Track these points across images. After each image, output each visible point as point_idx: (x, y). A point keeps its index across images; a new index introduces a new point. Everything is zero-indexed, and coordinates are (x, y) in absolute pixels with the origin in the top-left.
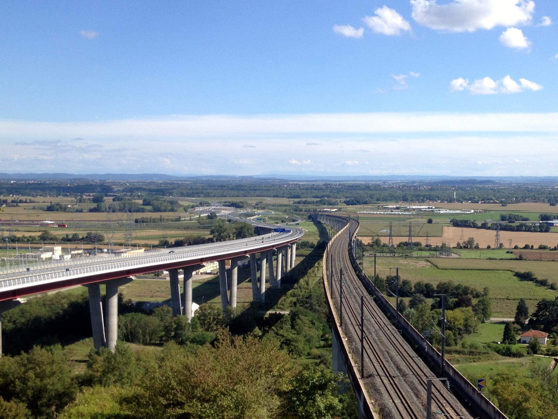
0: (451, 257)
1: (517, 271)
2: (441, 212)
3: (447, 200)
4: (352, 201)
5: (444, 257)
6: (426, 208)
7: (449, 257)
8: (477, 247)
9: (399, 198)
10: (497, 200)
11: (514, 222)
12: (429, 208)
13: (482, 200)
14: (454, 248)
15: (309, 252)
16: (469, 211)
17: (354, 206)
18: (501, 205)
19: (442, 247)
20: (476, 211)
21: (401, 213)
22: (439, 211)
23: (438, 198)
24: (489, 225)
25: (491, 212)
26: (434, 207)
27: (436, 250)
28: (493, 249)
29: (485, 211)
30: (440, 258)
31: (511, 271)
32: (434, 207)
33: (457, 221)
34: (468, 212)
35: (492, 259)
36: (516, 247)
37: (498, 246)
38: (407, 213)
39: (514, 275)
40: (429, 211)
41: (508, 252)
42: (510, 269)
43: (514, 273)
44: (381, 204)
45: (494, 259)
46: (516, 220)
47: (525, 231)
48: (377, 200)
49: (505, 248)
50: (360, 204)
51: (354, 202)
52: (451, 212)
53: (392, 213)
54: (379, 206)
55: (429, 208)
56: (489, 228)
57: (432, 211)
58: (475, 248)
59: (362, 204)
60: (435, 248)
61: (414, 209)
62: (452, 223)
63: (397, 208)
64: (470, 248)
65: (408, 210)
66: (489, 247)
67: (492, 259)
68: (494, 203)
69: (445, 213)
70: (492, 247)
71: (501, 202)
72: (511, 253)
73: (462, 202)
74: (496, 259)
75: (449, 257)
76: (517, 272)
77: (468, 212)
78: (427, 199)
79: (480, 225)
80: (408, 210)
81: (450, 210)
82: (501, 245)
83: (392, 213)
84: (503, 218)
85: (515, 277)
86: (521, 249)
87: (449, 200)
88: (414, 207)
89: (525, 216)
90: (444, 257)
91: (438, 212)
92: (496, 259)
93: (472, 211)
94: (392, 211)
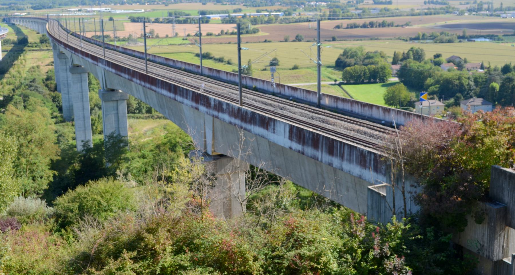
0: (138, 45)
3: (119, 3)
4: (38, 6)
5: (132, 45)
8: (157, 37)
9: (78, 3)
10: (160, 2)
11: (179, 17)
12: (106, 9)
13: (148, 2)
14: (138, 38)
15: (11, 48)
17: (41, 10)
18: (164, 5)
19: (128, 38)
21: (83, 14)
23: (111, 2)
24: (161, 20)
27: (124, 41)
29: (154, 10)
31: (191, 53)
32: (110, 9)
36: (188, 35)
37: (175, 34)
41: (183, 39)
43: (194, 55)
44: (64, 8)
46: (181, 16)
48: (60, 5)
49: (180, 37)
50: (45, 9)
51: (40, 7)
52: (126, 12)
53: (76, 14)
54: (62, 10)
55: (106, 9)
56: (161, 22)
57: (110, 12)
59: (48, 8)
60: (123, 39)
61: (94, 11)
62: (130, 20)
63: (80, 11)
64: (152, 38)
66: (167, 36)
68: (158, 4)
70: (170, 36)
71: (163, 3)
72: (186, 39)
73: (132, 4)
74: (176, 45)
75: (137, 45)
78: (102, 3)
79: (153, 20)
80: (89, 12)
81: (124, 10)
82: (177, 34)
84: (170, 14)
86: (192, 36)
87: (121, 3)
88: (94, 9)
89: (187, 12)
92: (176, 45)
93: (143, 11)
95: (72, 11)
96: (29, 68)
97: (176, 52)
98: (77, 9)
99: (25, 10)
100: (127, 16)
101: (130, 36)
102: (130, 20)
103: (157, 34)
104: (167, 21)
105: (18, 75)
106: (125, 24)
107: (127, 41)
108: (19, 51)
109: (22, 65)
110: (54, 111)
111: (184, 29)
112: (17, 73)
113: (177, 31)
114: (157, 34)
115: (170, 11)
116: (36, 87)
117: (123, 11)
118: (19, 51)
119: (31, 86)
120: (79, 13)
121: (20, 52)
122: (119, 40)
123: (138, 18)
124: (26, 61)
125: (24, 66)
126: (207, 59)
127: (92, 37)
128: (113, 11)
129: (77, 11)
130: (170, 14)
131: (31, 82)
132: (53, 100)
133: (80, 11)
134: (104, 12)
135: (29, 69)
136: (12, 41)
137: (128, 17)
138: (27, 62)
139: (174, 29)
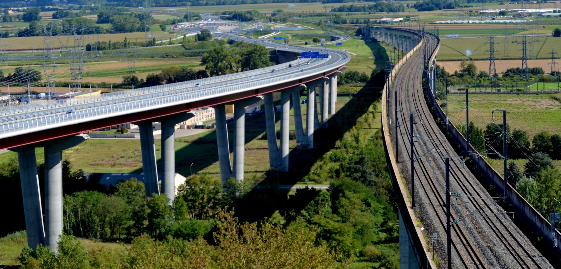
4: (427, 4)
6: (550, 12)
12: (555, 12)
15: (358, 89)
17: (431, 12)
21: (508, 21)
38: (518, 21)
50: (440, 9)
51: (431, 5)
53: (494, 21)
54: (471, 11)
55: (555, 12)
59: (444, 8)
61: (530, 15)
63: (502, 13)
65: (520, 16)
80: (520, 16)
83: (494, 21)
88: (530, 11)
94: (493, 19)
96: (376, 130)
98: (498, 12)
99: (403, 11)
105: (354, 144)
109: (366, 124)
112: (353, 139)
116: (364, 172)
119: (356, 171)
127: (508, 71)
129: (496, 14)
132: (390, 197)
133: (502, 13)
134: (549, 16)
136: (360, 75)
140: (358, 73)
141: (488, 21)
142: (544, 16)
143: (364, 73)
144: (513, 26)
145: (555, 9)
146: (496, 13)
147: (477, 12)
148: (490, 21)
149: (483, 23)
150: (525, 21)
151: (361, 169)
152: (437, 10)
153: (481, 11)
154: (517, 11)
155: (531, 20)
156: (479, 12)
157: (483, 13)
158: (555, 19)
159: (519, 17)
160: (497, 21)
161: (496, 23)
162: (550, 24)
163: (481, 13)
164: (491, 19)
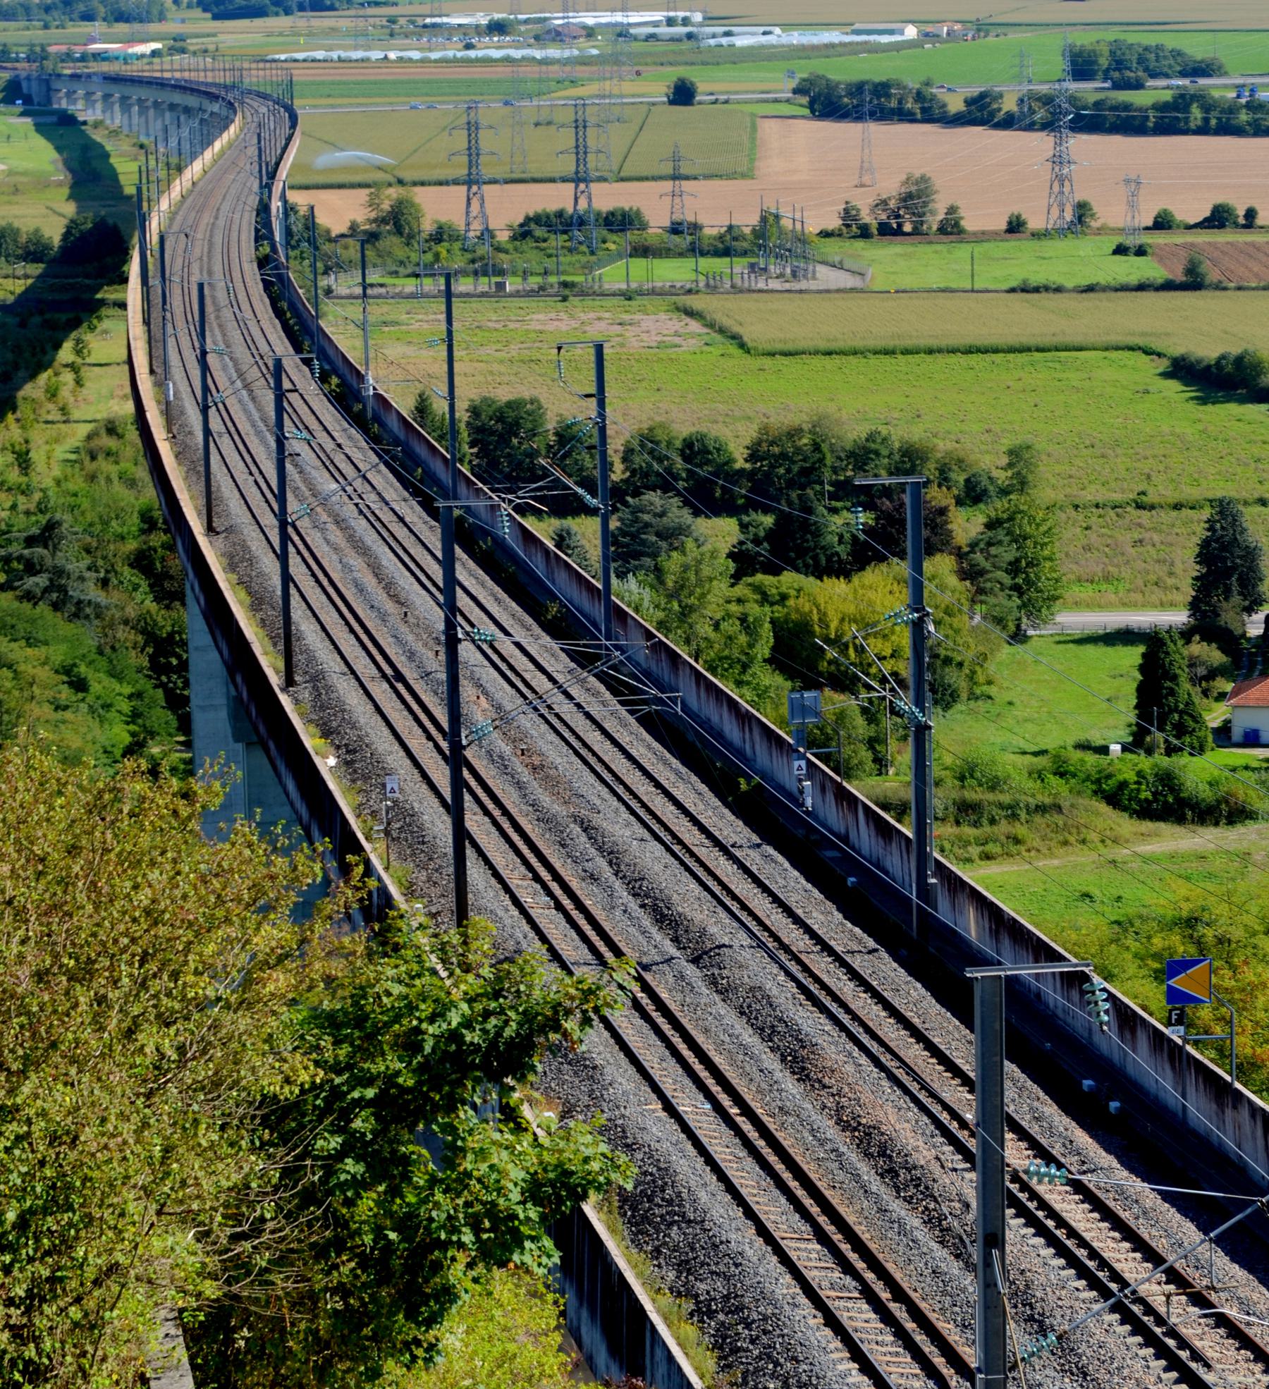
0: (813, 285)
1: (1178, 350)
2: (740, 42)
5: (775, 284)
6: (656, 24)
7: (803, 285)
8: (951, 229)
11: (1139, 86)
12: (670, 22)
14: (825, 234)
15: (19, 286)
16: (891, 32)
17: (258, 22)
20: (929, 28)
21: (517, 54)
22: (728, 34)
24: (1009, 104)
25: (1014, 37)
26: (698, 17)
27: (726, 252)
28: (1036, 235)
30: (750, 291)
31: (1148, 352)
32: (698, 17)
33: (831, 87)
34: (885, 39)
35: (1036, 290)
36: (1162, 223)
37: (1068, 216)
38: (553, 52)
39: (1166, 375)
40: (674, 39)
41: (1120, 250)
42: (1140, 341)
43: (1164, 365)
45: (1047, 289)
46: (1154, 75)
47: (1203, 130)
49: (1100, 231)
50: (288, 12)
52: (796, 38)
53: (472, 54)
54: (392, 20)
55: (670, 22)
56: (1008, 123)
57: (690, 36)
58: (942, 230)
60: (721, 238)
61: (590, 32)
62: (805, 100)
63: (498, 28)
64: (916, 232)
65: (558, 36)
66: (1015, 227)
67: (1036, 290)
69: (763, 47)
70: (1035, 222)
72: (1141, 252)
74: (1059, 290)
75: (803, 285)
76: (1183, 358)
77: (885, 39)
79: (955, 104)
80: (558, 36)
81: (787, 26)
82: (1082, 212)
83: (472, 54)
84: (1082, 67)
85: (1174, 386)
86: (1189, 227)
88: (589, 19)
89: (1197, 48)
90: (775, 284)
91: (724, 41)
92: (1059, 290)
93: (911, 32)
94: (469, 47)
95: (451, 30)
96: (90, 427)
97: (1047, 341)
98: (484, 21)
100: (791, 74)
101: (768, 221)
102: (805, 100)
103: (952, 210)
104: (1041, 114)
106: (769, 129)
107: (745, 253)
108: (56, 306)
109: (51, 406)
110: (152, 734)
111: (1127, 181)
112: (10, 458)
113: (1079, 197)
114: (952, 210)
115: (1084, 39)
116: (59, 572)
117: (778, 37)
118: (56, 306)
119: (31, 568)
120: (492, 49)
121: (63, 317)
122: (695, 250)
123: (858, 89)
124: (79, 382)
125: (63, 410)
126: (1242, 400)
127: (528, 220)
128: (712, 36)
130: (1082, 67)
131: (30, 541)
132: (152, 658)
133: (498, 28)
135: (89, 437)
136: (23, 239)
137: (793, 84)
138: (90, 389)
139: (1061, 180)
140: (17, 232)
141: (450, 54)
142: (635, 38)
143: (37, 231)
144: (536, 69)
145: (672, 14)
146: (477, 26)
147: (413, 22)
148: (459, 54)
149: (436, 61)
150: (576, 52)
151: (49, 562)
152: (277, 14)
153: (428, 20)
154: (545, 19)
155: (595, 52)
156: (420, 22)
157: (434, 25)
158: (673, 47)
159: (554, 40)
160: (480, 53)
161: (477, 60)
162: (655, 64)
163: (425, 26)
164: (461, 45)
